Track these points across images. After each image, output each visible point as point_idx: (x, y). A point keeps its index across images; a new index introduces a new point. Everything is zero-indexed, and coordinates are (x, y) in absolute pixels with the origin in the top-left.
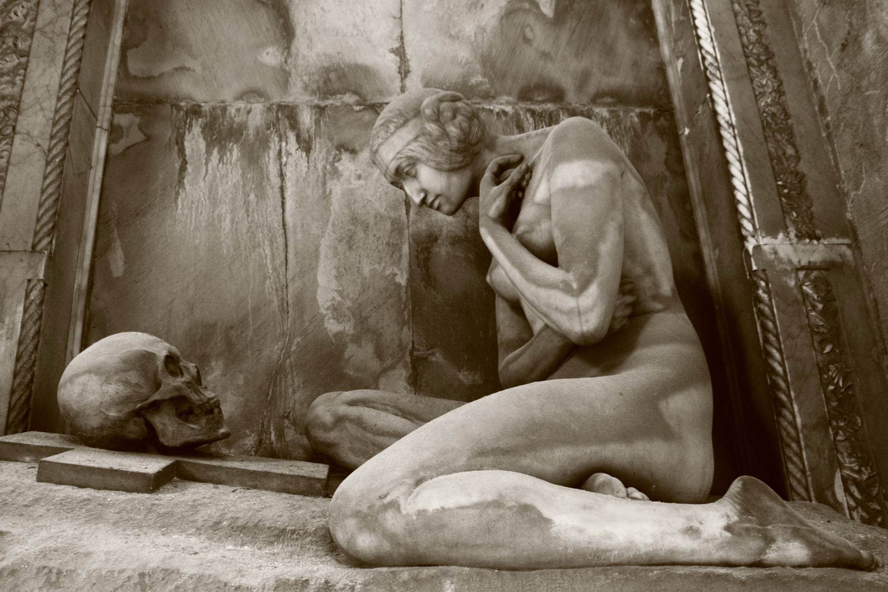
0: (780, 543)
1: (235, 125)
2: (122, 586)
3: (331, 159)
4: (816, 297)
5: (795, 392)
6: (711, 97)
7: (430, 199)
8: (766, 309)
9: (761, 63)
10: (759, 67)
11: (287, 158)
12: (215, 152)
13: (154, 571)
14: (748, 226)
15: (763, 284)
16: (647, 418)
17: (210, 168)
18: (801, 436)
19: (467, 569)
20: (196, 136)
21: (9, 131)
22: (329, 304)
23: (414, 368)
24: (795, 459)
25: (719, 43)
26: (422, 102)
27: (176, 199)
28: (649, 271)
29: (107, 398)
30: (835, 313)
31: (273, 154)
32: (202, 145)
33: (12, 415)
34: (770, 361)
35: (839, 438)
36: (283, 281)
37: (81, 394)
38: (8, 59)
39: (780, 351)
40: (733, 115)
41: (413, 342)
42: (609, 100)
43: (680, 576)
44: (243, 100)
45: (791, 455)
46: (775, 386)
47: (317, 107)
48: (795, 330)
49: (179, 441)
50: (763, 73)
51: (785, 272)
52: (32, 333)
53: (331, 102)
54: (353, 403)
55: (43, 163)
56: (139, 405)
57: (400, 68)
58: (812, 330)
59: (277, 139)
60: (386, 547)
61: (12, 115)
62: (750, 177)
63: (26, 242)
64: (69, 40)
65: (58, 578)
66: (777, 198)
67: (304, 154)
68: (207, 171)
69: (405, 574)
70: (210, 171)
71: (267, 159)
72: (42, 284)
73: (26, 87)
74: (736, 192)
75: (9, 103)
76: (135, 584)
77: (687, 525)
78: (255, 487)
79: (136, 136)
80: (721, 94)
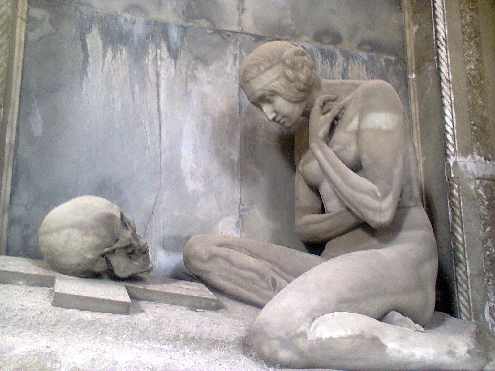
1: (124, 32)
3: (191, 67)
4: (484, 196)
5: (468, 254)
6: (438, 59)
8: (457, 202)
9: (471, 39)
10: (469, 41)
12: (110, 50)
15: (456, 186)
17: (106, 62)
18: (469, 281)
20: (95, 35)
22: (188, 170)
23: (241, 216)
24: (465, 294)
25: (448, 23)
31: (151, 57)
32: (100, 43)
34: (456, 234)
35: (490, 283)
36: (158, 150)
37: (66, 241)
39: (462, 228)
40: (450, 74)
41: (241, 200)
42: (368, 47)
44: (129, 12)
45: (462, 291)
46: (456, 249)
47: (182, 26)
49: (126, 275)
51: (469, 180)
53: (191, 24)
57: (238, 5)
58: (481, 217)
59: (154, 47)
60: (296, 358)
62: (456, 118)
67: (173, 61)
68: (104, 64)
71: (147, 61)
78: (174, 304)
80: (445, 58)
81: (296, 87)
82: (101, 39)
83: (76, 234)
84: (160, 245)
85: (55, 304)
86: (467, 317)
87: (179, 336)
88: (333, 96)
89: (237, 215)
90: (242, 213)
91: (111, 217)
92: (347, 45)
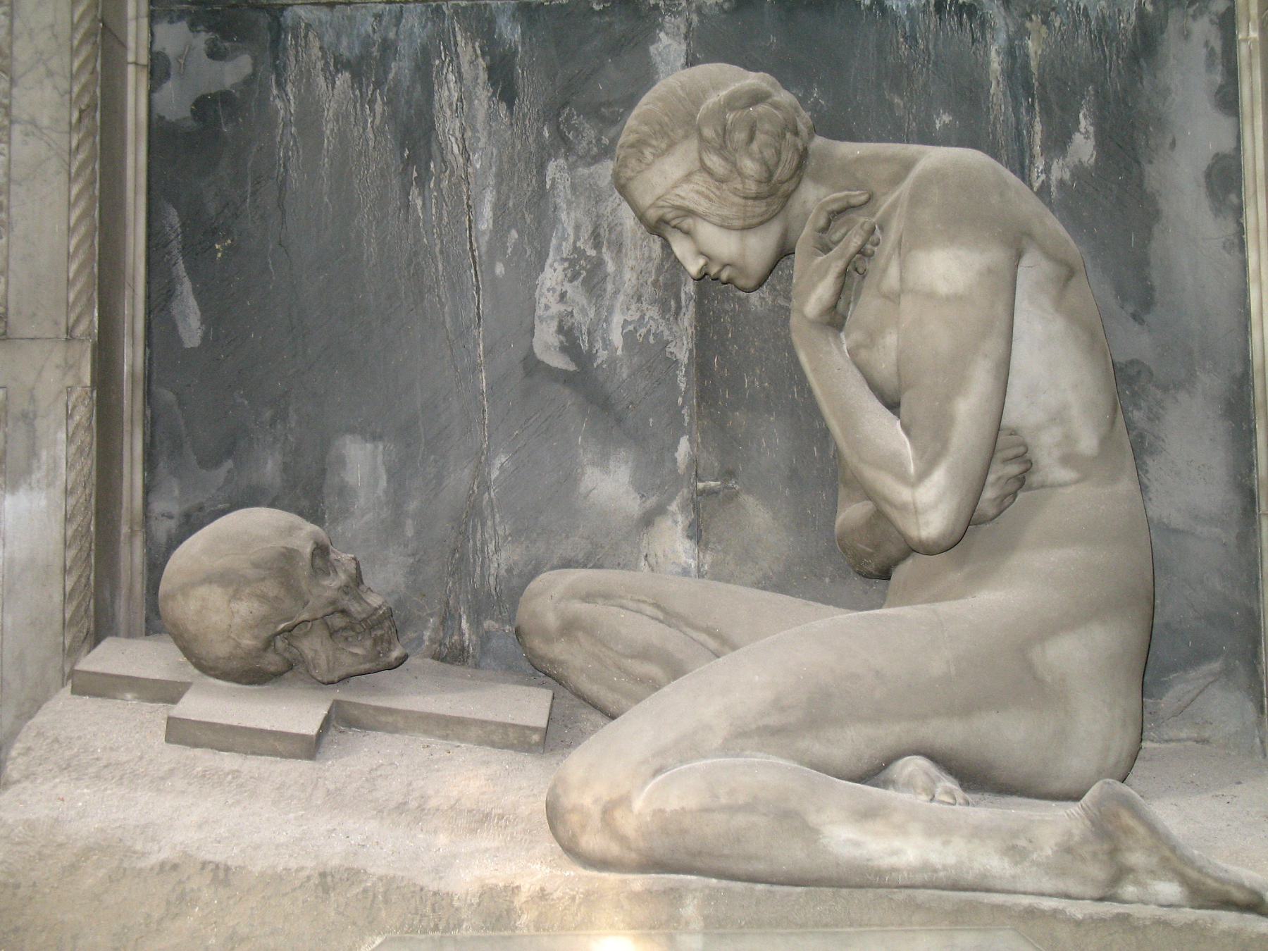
16: (1012, 673)
26: (697, 103)
29: (237, 620)
54: (588, 597)
55: (63, 177)
63: (56, 323)
65: (226, 875)
76: (317, 886)
81: (735, 192)
83: (215, 596)
87: (405, 803)
88: (858, 197)
91: (289, 556)
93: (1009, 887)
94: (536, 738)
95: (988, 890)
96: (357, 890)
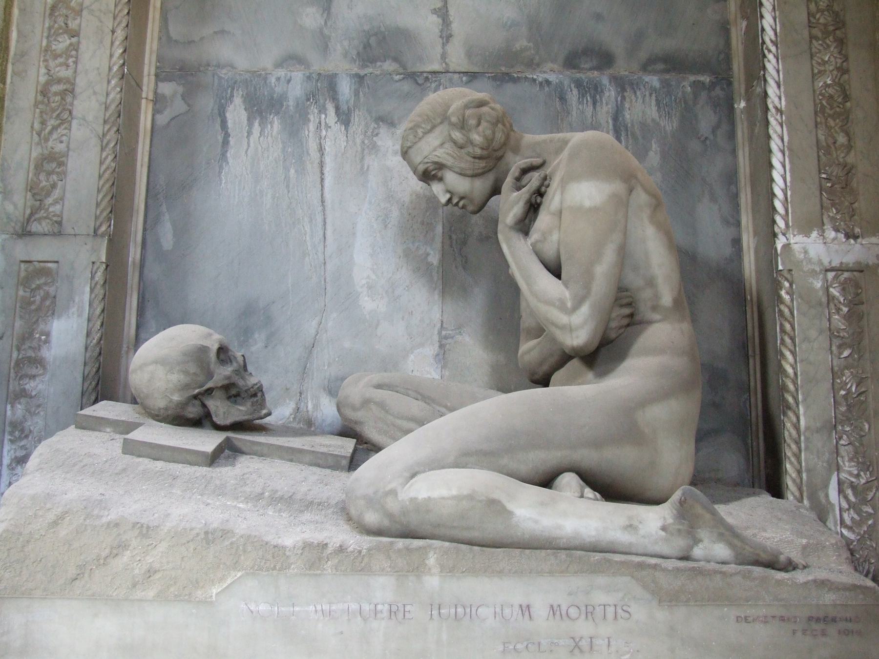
0: (706, 543)
1: (275, 96)
2: (192, 540)
3: (369, 133)
4: (842, 300)
5: (803, 394)
6: (764, 75)
7: (455, 201)
8: (786, 311)
10: (824, 39)
11: (327, 131)
12: (256, 124)
13: (215, 530)
14: (780, 222)
15: (787, 284)
18: (802, 438)
19: (447, 544)
21: (65, 115)
22: (364, 282)
23: (441, 346)
26: (449, 107)
27: (220, 173)
28: (651, 283)
29: (171, 385)
30: (860, 318)
32: (244, 115)
33: (86, 385)
34: (783, 363)
38: (60, 40)
39: (794, 353)
40: (783, 99)
43: (616, 562)
47: (357, 76)
48: (813, 333)
49: (228, 422)
50: (828, 46)
51: (813, 273)
52: (99, 310)
53: (371, 70)
54: (379, 386)
55: (99, 148)
56: (197, 391)
57: (441, 31)
58: (832, 333)
59: (316, 111)
60: (386, 523)
61: (69, 99)
64: (115, 18)
65: (148, 531)
66: (817, 193)
67: (343, 128)
68: (248, 144)
69: (401, 543)
70: (252, 144)
71: (307, 132)
72: (104, 266)
73: (78, 71)
74: (774, 185)
75: (65, 87)
76: (202, 539)
77: (627, 523)
78: (291, 461)
79: (179, 106)
81: (468, 154)
82: (245, 109)
84: (324, 390)
85: (125, 452)
86: (795, 496)
88: (537, 161)
89: (437, 345)
90: (444, 342)
91: (203, 350)
92: (622, 68)
93: (627, 550)
94: (345, 463)
95: (614, 552)
96: (227, 543)
